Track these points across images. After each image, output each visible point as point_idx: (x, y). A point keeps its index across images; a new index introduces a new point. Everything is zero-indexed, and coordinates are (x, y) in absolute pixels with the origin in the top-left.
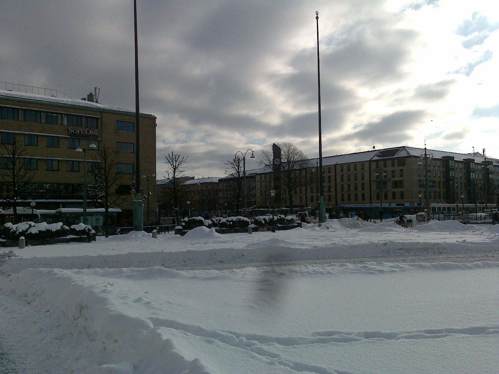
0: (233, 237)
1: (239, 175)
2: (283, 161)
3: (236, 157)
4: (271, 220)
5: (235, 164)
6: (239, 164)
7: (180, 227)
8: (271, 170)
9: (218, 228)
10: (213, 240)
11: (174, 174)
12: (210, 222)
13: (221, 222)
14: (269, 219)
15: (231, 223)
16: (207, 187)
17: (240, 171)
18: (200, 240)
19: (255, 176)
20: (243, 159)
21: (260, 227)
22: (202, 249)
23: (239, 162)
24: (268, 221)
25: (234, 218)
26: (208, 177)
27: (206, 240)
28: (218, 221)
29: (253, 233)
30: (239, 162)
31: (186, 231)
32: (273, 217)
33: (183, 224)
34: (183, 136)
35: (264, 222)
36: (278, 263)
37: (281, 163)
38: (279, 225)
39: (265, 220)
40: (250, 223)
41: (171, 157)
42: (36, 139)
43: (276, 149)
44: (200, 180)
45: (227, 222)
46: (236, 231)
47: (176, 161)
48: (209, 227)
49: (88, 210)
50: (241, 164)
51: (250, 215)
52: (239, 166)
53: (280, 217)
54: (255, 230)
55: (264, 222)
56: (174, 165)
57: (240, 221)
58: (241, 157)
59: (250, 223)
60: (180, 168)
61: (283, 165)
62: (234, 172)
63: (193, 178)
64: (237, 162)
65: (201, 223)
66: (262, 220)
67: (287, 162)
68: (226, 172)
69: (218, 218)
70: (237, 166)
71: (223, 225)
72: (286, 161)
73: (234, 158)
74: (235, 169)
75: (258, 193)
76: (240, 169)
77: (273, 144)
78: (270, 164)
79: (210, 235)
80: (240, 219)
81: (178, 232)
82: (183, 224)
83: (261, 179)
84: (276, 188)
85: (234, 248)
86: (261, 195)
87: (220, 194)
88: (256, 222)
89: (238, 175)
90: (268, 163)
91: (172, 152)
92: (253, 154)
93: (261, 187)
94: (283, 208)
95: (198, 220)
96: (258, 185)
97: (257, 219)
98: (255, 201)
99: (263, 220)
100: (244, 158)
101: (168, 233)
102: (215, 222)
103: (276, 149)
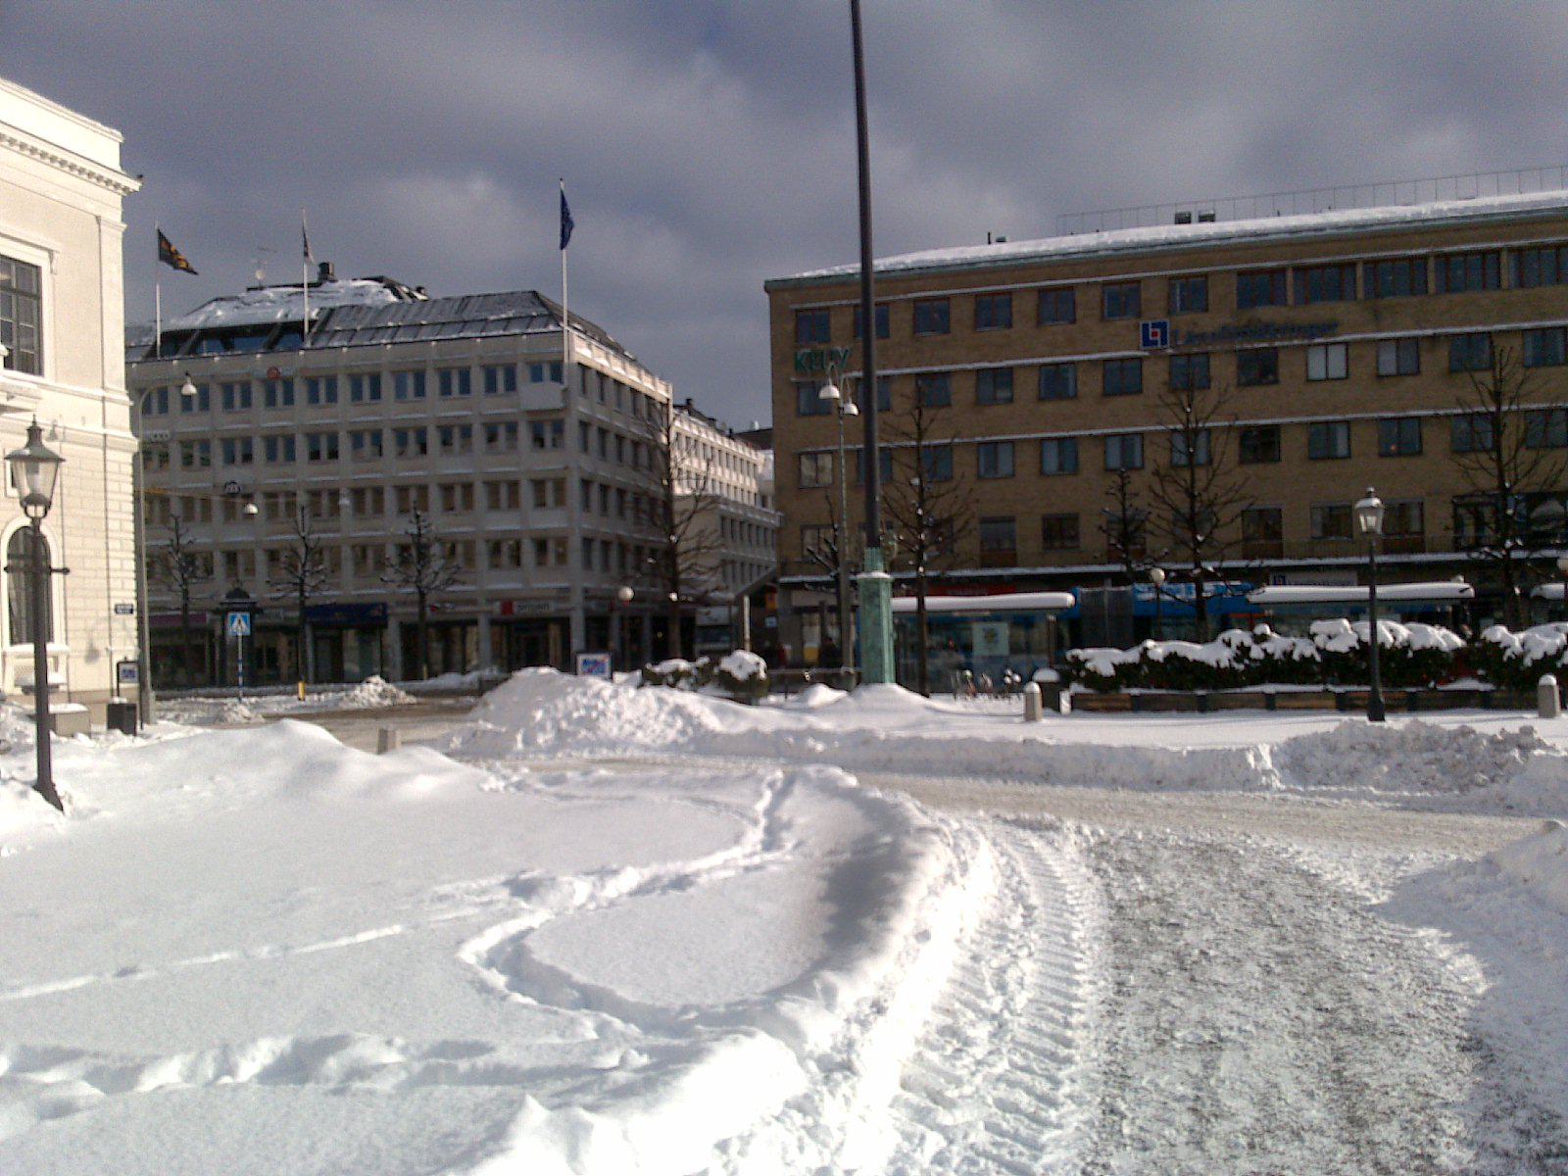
49: (1382, 591)
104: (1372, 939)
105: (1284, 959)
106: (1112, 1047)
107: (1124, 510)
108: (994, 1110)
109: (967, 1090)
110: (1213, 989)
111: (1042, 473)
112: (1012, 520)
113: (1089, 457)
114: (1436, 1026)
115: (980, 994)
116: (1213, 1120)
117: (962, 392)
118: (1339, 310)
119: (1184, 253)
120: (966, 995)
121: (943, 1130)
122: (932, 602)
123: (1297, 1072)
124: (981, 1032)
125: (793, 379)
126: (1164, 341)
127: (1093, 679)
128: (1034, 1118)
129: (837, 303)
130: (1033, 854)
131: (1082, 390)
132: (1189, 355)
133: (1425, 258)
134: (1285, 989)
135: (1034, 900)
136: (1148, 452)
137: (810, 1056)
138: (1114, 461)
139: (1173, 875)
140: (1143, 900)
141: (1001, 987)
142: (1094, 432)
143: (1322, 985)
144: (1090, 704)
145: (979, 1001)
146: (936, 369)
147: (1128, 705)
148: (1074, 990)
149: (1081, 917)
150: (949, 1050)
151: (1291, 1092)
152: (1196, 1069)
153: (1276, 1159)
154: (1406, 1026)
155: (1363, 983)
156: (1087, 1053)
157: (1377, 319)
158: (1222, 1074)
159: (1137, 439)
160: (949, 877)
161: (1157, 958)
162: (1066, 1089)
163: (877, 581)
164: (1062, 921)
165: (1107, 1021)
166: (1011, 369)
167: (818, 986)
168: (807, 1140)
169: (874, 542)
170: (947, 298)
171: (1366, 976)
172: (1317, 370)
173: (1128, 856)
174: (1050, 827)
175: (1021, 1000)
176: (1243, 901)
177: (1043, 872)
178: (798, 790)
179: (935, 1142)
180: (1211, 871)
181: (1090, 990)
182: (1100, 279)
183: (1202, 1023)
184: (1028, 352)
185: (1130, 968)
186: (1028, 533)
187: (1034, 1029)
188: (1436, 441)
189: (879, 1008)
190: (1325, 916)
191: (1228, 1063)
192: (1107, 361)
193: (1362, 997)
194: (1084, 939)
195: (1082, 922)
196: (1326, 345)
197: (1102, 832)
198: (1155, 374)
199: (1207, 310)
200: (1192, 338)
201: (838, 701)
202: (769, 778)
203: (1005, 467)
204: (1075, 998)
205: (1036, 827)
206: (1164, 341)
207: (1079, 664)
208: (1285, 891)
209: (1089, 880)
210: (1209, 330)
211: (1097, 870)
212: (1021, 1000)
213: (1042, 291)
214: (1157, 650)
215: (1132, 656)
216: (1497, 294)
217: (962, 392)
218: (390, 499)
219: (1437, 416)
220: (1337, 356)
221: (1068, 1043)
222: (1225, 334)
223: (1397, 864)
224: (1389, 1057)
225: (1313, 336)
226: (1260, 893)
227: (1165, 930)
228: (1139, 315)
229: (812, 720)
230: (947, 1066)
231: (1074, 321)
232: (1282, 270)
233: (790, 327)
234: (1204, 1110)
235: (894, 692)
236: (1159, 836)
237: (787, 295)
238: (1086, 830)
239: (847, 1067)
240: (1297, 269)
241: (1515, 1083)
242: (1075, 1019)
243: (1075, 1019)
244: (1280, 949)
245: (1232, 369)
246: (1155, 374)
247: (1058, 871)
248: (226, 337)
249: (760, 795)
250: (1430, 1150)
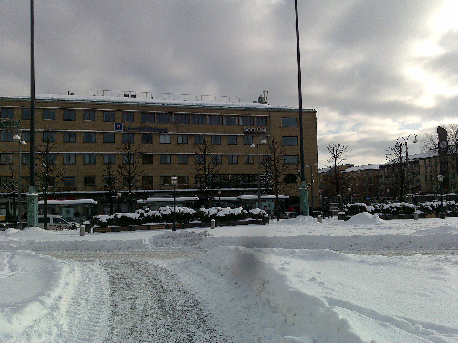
0: (398, 224)
1: (401, 161)
2: (451, 144)
3: (397, 143)
4: (440, 207)
5: (396, 150)
6: (401, 150)
7: (344, 213)
8: (436, 154)
9: (381, 214)
10: (376, 226)
11: (335, 162)
12: (373, 208)
13: (384, 208)
14: (437, 206)
15: (395, 209)
16: (368, 174)
17: (402, 156)
18: (364, 226)
19: (418, 161)
20: (405, 144)
21: (426, 213)
22: (367, 235)
23: (400, 148)
24: (171, 213)
25: (398, 205)
26: (369, 164)
27: (369, 225)
28: (381, 207)
29: (419, 219)
30: (400, 148)
31: (349, 216)
32: (442, 203)
33: (346, 210)
34: (334, 127)
35: (431, 208)
36: (451, 251)
37: (448, 146)
38: (449, 212)
39: (432, 206)
40: (416, 210)
41: (332, 147)
42: (85, 140)
43: (442, 132)
44: (361, 167)
45: (390, 208)
46: (401, 218)
47: (337, 150)
48: (372, 213)
49: (177, 199)
50: (404, 149)
51: (415, 201)
52: (401, 151)
53: (449, 203)
54: (422, 216)
55: (431, 208)
56: (335, 154)
57: (404, 207)
58: (403, 143)
59: (416, 210)
60: (341, 157)
61: (451, 148)
62: (395, 157)
63: (353, 166)
64: (399, 147)
65: (364, 209)
66: (428, 206)
67: (455, 144)
68: (387, 159)
69: (381, 204)
70: (399, 152)
71: (386, 211)
72: (453, 143)
73: (396, 144)
74: (397, 155)
75: (423, 178)
76: (402, 154)
77: (438, 127)
78: (435, 148)
79: (373, 221)
80: (404, 206)
81: (341, 217)
82: (346, 210)
83: (425, 164)
84: (442, 172)
85: (401, 234)
86: (426, 180)
87: (382, 180)
88: (422, 208)
89: (400, 160)
90: (432, 146)
91: (333, 142)
92: (415, 138)
93: (426, 172)
94: (452, 194)
95: (360, 206)
96: (422, 170)
97: (423, 205)
98: (420, 187)
99: (430, 206)
100: (406, 143)
101: (332, 218)
102: (378, 208)
103: (442, 132)
104: (168, 276)
105: (150, 282)
106: (113, 301)
107: (109, 176)
108: (89, 314)
109: (82, 312)
110: (135, 289)
111: (84, 164)
112: (74, 177)
113: (99, 160)
114: (179, 290)
115: (82, 295)
116: (135, 309)
117: (59, 138)
119: (127, 105)
120: (78, 296)
121: (78, 318)
122: (49, 202)
123: (152, 300)
124: (83, 302)
126: (121, 129)
127: (101, 223)
128: (98, 314)
130: (90, 268)
131: (97, 141)
132: (128, 133)
133: (189, 115)
134: (150, 287)
135: (90, 277)
136: (117, 160)
137: (47, 307)
138: (107, 160)
139: (124, 269)
140: (118, 274)
141: (86, 294)
142: (100, 153)
143: (157, 286)
144: (99, 230)
145: (81, 297)
146: (50, 130)
147: (110, 230)
148: (103, 293)
149: (103, 279)
150: (76, 306)
151: (150, 302)
152: (131, 302)
153: (147, 313)
154: (173, 290)
155: (166, 284)
156: (108, 303)
157: (177, 129)
158: (136, 303)
159: (113, 155)
160: (70, 272)
161: (122, 285)
162: (104, 309)
163: (33, 196)
164: (98, 280)
165: (111, 297)
166: (75, 132)
167: (46, 294)
168: (51, 320)
169: (32, 184)
170: (55, 109)
171: (166, 283)
172: (162, 141)
173: (113, 266)
174: (92, 261)
175: (91, 295)
176: (141, 272)
177: (93, 271)
178: (16, 256)
179: (77, 320)
180: (133, 267)
181: (107, 291)
182: (103, 110)
183: (132, 295)
184: (81, 128)
185: (116, 288)
186: (79, 181)
187: (95, 300)
189: (60, 298)
190: (159, 274)
191: (138, 301)
192: (104, 133)
193: (165, 287)
194: (104, 283)
195: (103, 280)
196: (165, 134)
197: (106, 261)
198: (119, 138)
199: (133, 122)
200: (129, 129)
201: (18, 232)
202: (6, 254)
203: (72, 161)
204: (104, 294)
205: (90, 261)
206: (121, 129)
207: (97, 219)
208: (150, 270)
209: (104, 272)
210: (134, 127)
211: (105, 270)
212: (91, 295)
213: (85, 111)
214: (119, 215)
215: (112, 217)
216: (205, 126)
217: (59, 138)
220: (168, 137)
221: (103, 302)
222: (138, 129)
223: (175, 262)
224: (169, 296)
225: (162, 132)
226: (145, 271)
227: (123, 280)
228: (114, 121)
229: (10, 238)
230: (77, 308)
231: (95, 121)
232: (154, 113)
234: (133, 309)
235: (37, 229)
236: (120, 261)
238: (102, 261)
239: (57, 308)
240: (157, 113)
241: (191, 296)
242: (104, 297)
243: (104, 297)
244: (149, 280)
245: (140, 139)
246: (119, 138)
247: (96, 270)
249: (5, 259)
250: (175, 308)
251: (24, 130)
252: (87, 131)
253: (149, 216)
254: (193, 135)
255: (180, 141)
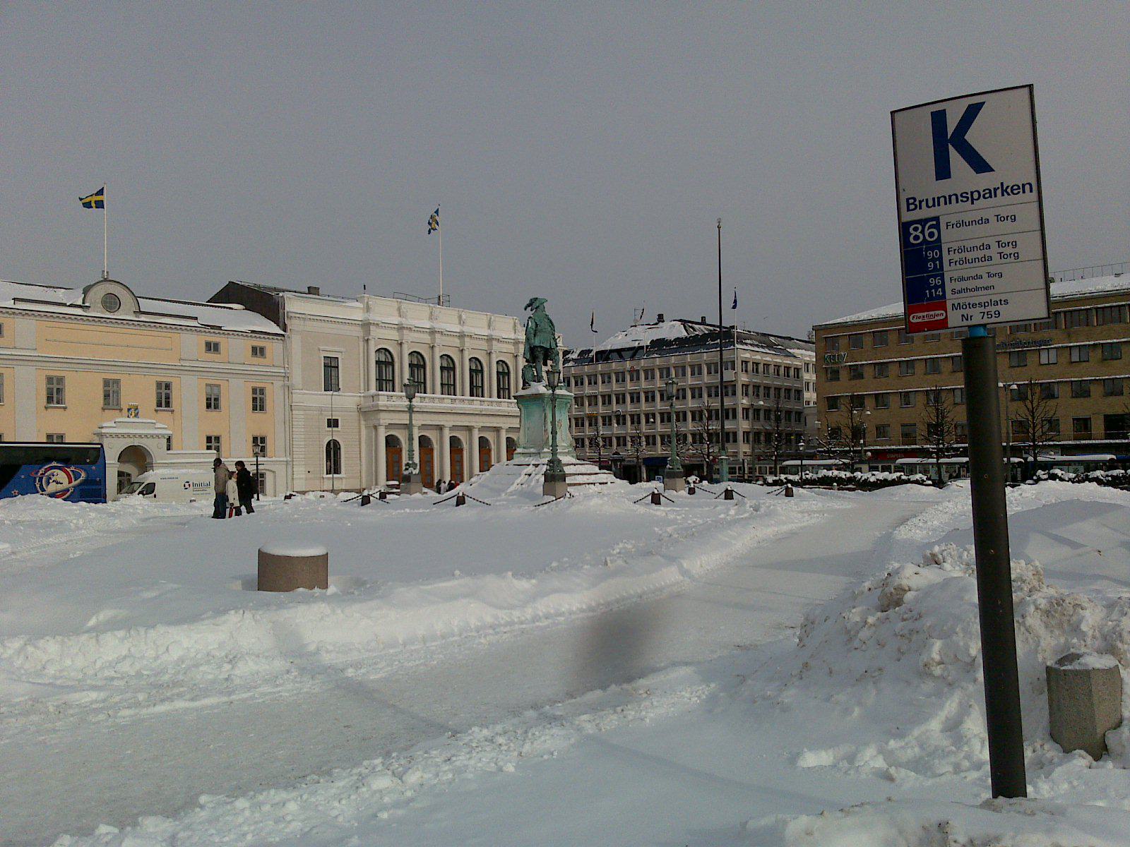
118: (1053, 333)
125: (824, 366)
129: (841, 334)
133: (1090, 309)
146: (881, 361)
157: (1069, 337)
172: (1044, 360)
188: (1096, 391)
192: (952, 357)
196: (1048, 349)
218: (689, 416)
219: (1095, 379)
220: (1053, 353)
225: (1041, 346)
233: (823, 344)
237: (822, 332)
248: (620, 352)
251: (852, 363)
252: (928, 357)
253: (807, 478)
254: (1097, 344)
255: (1075, 358)
